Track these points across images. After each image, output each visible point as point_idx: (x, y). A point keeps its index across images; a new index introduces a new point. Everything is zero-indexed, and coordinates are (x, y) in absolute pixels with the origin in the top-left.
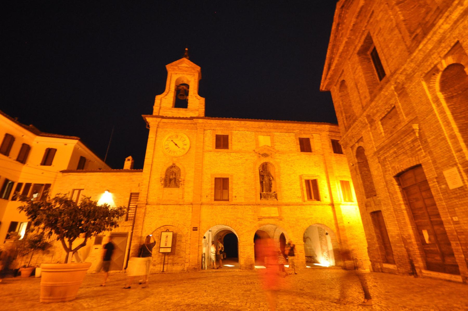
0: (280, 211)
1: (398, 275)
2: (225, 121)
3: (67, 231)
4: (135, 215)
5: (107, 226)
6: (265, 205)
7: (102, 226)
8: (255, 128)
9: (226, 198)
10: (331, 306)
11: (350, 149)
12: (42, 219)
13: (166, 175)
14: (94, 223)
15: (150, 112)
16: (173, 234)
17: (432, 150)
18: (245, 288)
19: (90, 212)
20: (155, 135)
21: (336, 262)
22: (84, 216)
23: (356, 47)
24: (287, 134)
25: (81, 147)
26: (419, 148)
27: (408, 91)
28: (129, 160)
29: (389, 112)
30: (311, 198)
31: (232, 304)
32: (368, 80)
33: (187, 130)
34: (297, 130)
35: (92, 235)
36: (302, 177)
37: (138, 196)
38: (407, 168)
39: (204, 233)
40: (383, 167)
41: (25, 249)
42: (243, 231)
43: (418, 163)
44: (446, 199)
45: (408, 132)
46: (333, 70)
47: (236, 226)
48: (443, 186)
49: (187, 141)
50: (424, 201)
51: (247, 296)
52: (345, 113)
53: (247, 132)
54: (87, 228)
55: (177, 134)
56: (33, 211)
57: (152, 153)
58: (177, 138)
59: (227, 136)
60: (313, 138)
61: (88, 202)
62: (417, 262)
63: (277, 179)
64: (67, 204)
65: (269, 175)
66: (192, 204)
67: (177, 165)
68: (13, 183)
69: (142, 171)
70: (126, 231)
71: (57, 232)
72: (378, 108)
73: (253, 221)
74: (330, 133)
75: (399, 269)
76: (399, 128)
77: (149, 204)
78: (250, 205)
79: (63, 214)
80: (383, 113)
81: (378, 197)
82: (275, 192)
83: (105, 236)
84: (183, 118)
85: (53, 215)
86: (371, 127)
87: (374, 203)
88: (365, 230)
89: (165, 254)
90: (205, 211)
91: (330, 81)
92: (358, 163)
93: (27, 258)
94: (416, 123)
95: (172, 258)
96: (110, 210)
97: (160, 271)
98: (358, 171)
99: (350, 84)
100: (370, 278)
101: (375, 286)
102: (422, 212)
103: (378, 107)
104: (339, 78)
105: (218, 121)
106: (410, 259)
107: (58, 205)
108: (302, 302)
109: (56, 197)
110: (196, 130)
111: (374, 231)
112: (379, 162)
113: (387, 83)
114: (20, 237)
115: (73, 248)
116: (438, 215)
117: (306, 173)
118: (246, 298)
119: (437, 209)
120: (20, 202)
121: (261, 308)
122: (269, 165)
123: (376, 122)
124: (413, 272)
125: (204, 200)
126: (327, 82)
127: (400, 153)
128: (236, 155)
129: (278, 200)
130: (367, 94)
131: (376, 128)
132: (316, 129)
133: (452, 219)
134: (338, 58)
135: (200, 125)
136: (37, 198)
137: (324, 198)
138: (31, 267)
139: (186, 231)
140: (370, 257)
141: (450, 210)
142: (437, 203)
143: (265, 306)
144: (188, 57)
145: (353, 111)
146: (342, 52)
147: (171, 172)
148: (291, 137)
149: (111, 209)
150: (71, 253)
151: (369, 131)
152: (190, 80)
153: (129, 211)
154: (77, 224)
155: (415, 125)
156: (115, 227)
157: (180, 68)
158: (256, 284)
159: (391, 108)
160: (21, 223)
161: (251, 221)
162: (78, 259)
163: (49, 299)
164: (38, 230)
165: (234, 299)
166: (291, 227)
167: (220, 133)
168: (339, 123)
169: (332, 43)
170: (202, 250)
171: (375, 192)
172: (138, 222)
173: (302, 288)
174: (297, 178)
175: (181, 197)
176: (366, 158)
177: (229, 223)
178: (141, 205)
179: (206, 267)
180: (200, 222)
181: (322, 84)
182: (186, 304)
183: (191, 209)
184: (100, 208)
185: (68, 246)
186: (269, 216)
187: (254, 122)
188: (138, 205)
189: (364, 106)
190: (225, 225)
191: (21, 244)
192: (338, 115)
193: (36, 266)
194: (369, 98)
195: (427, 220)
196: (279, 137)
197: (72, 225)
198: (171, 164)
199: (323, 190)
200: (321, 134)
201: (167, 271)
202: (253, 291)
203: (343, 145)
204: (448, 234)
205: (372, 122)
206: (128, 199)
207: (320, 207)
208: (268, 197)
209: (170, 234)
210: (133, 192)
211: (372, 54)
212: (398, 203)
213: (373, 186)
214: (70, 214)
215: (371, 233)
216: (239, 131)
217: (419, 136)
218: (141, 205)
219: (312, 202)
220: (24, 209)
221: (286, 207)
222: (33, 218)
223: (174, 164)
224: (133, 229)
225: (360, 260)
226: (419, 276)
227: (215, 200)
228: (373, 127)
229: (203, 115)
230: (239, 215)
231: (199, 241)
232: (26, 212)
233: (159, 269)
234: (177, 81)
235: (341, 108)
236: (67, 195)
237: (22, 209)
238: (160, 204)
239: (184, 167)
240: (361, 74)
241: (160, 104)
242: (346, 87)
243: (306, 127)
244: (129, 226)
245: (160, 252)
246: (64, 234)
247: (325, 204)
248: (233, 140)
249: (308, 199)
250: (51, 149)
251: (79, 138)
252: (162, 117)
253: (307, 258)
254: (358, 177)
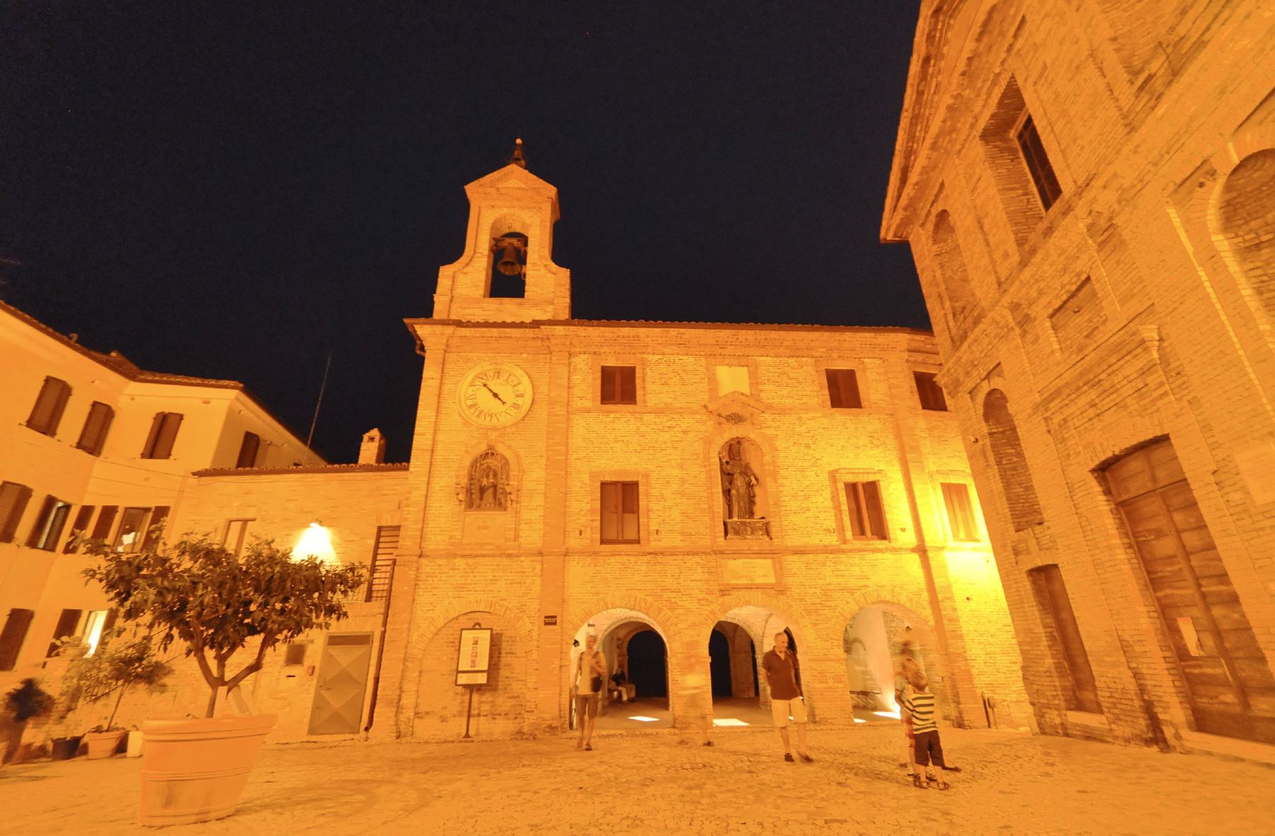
117: (847, 466)
128: (658, 420)
137: (899, 532)
186: (750, 582)
219: (866, 542)
249: (854, 535)
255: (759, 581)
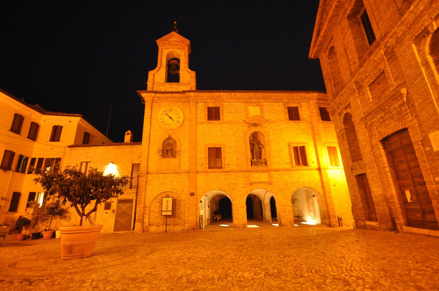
0: (270, 177)
1: (380, 231)
2: (216, 93)
3: (79, 199)
4: (138, 183)
5: (114, 194)
6: (256, 171)
7: (108, 193)
8: (244, 99)
9: (220, 166)
10: (316, 258)
11: (338, 116)
12: (56, 189)
13: (163, 147)
14: (102, 191)
15: (144, 88)
16: (173, 199)
17: (419, 113)
18: (238, 244)
19: (97, 181)
20: (151, 109)
21: (322, 221)
22: (92, 185)
23: (346, 10)
24: (276, 104)
25: (84, 123)
26: (406, 112)
27: (398, 55)
28: (128, 134)
29: (378, 78)
30: (299, 164)
31: (227, 257)
32: (358, 45)
33: (180, 103)
34: (285, 100)
35: (101, 201)
36: (291, 144)
37: (139, 167)
38: (393, 132)
39: (201, 197)
40: (369, 132)
41: (44, 215)
42: (236, 195)
43: (404, 127)
44: (430, 161)
45: (396, 97)
46: (323, 36)
47: (229, 191)
48: (428, 149)
49: (181, 114)
50: (408, 163)
51: (240, 251)
52: (334, 80)
53: (237, 103)
54: (96, 196)
55: (171, 108)
56: (47, 182)
57: (149, 127)
58: (171, 111)
59: (219, 108)
60: (301, 107)
61: (95, 173)
62: (399, 219)
63: (267, 148)
64: (77, 175)
65: (259, 143)
66: (188, 172)
67: (173, 137)
68: (27, 158)
69: (141, 144)
70: (131, 198)
71: (70, 200)
72: (367, 74)
73: (245, 186)
74: (319, 100)
75: (381, 225)
76: (387, 93)
77: (150, 174)
78: (242, 172)
79: (74, 184)
80: (372, 78)
81: (364, 161)
82: (265, 159)
83: (113, 202)
84: (176, 93)
85: (66, 185)
86: (359, 93)
87: (360, 166)
88: (350, 192)
89: (167, 216)
90: (201, 179)
91: (319, 48)
92: (345, 129)
93: (47, 223)
94: (404, 88)
95: (173, 220)
96: (115, 179)
97: (163, 231)
98: (345, 137)
99: (339, 50)
100: (353, 234)
101: (357, 241)
102: (406, 173)
103: (367, 72)
104: (328, 45)
105: (209, 94)
106: (391, 217)
107: (68, 177)
108: (289, 255)
109: (66, 170)
110: (189, 104)
111: (358, 192)
112: (366, 127)
113: (376, 47)
114: (39, 205)
115: (86, 213)
116: (421, 176)
117: (294, 141)
118: (239, 252)
119: (421, 170)
120: (35, 174)
121: (252, 260)
122: (259, 134)
123: (364, 88)
124: (394, 228)
125: (199, 168)
126: (315, 49)
127: (387, 118)
128: (228, 126)
129: (268, 167)
130: (356, 60)
131: (364, 94)
132: (305, 98)
133: (434, 180)
134: (327, 24)
135: (192, 98)
136: (50, 170)
137: (312, 163)
138: (52, 230)
139: (184, 196)
140: (353, 216)
141: (433, 171)
142: (420, 165)
143: (257, 258)
144: (177, 31)
145: (342, 78)
146: (332, 17)
147: (168, 144)
148: (280, 106)
149: (116, 179)
150: (84, 218)
151: (357, 97)
152: (180, 54)
153: (133, 180)
154: (86, 192)
155: (404, 89)
156: (121, 194)
157: (170, 42)
158: (248, 241)
159: (380, 73)
160: (39, 193)
161: (243, 186)
162: (91, 223)
163: (69, 256)
164: (53, 199)
165: (229, 253)
166: (280, 191)
167: (211, 105)
168: (328, 91)
169: (321, 7)
170: (199, 213)
171: (361, 156)
172: (141, 189)
173: (289, 243)
174: (286, 145)
175: (178, 166)
176: (353, 124)
177: (223, 189)
178: (143, 174)
179: (204, 227)
180: (196, 188)
181: (310, 52)
182: (187, 258)
183: (188, 177)
184: (106, 178)
185: (81, 212)
187: (243, 94)
188: (140, 175)
189: (353, 72)
190: (219, 190)
191: (41, 211)
192: (327, 82)
193: (56, 230)
194: (358, 64)
195: (409, 181)
196: (268, 107)
197: (83, 194)
198: (167, 136)
199: (311, 156)
200: (309, 102)
201: (169, 231)
202: (246, 246)
203: (330, 112)
204: (429, 194)
205: (360, 88)
206: (131, 169)
207: (308, 172)
208: (258, 163)
209: (170, 200)
210: (134, 163)
211: (362, 17)
212: (383, 166)
213: (359, 150)
214: (81, 184)
215: (356, 194)
216: (229, 102)
217: (406, 101)
218: (143, 174)
219: (300, 167)
220: (39, 181)
221: (276, 172)
222: (48, 188)
223: (169, 136)
224: (137, 196)
225: (345, 218)
226: (400, 232)
227: (209, 168)
228: (361, 93)
229: (194, 88)
230: (232, 181)
231: (197, 205)
232: (41, 183)
233: (162, 229)
234: (168, 56)
235: (329, 75)
236: (76, 167)
237: (38, 181)
238: (159, 173)
239: (179, 139)
240: (351, 39)
241: (153, 80)
242: (335, 54)
243: (294, 96)
244: (133, 193)
245: (163, 214)
246: (77, 201)
247: (312, 169)
248: (224, 111)
249: (296, 164)
250: (58, 126)
251: (81, 115)
252: (156, 92)
253: (295, 217)
254: (344, 143)
255: (263, 180)
